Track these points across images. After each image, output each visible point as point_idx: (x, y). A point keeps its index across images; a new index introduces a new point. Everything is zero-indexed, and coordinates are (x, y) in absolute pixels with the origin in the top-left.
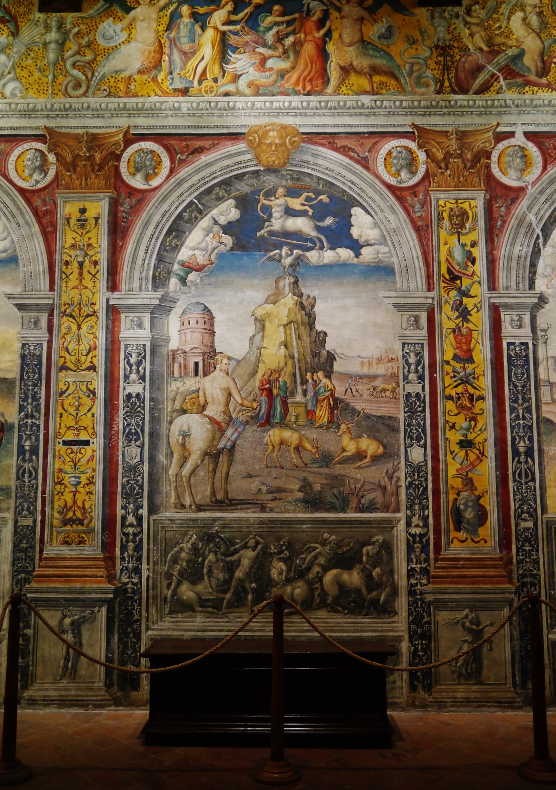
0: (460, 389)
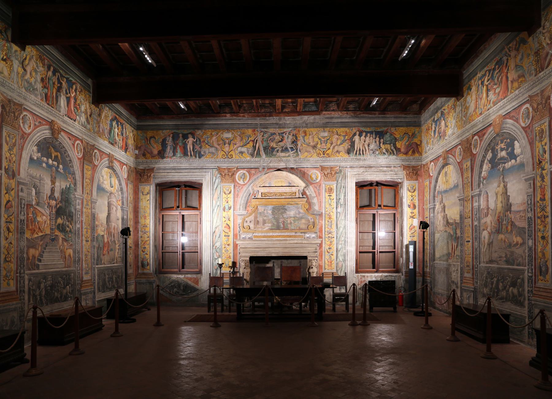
0: (541, 214)
